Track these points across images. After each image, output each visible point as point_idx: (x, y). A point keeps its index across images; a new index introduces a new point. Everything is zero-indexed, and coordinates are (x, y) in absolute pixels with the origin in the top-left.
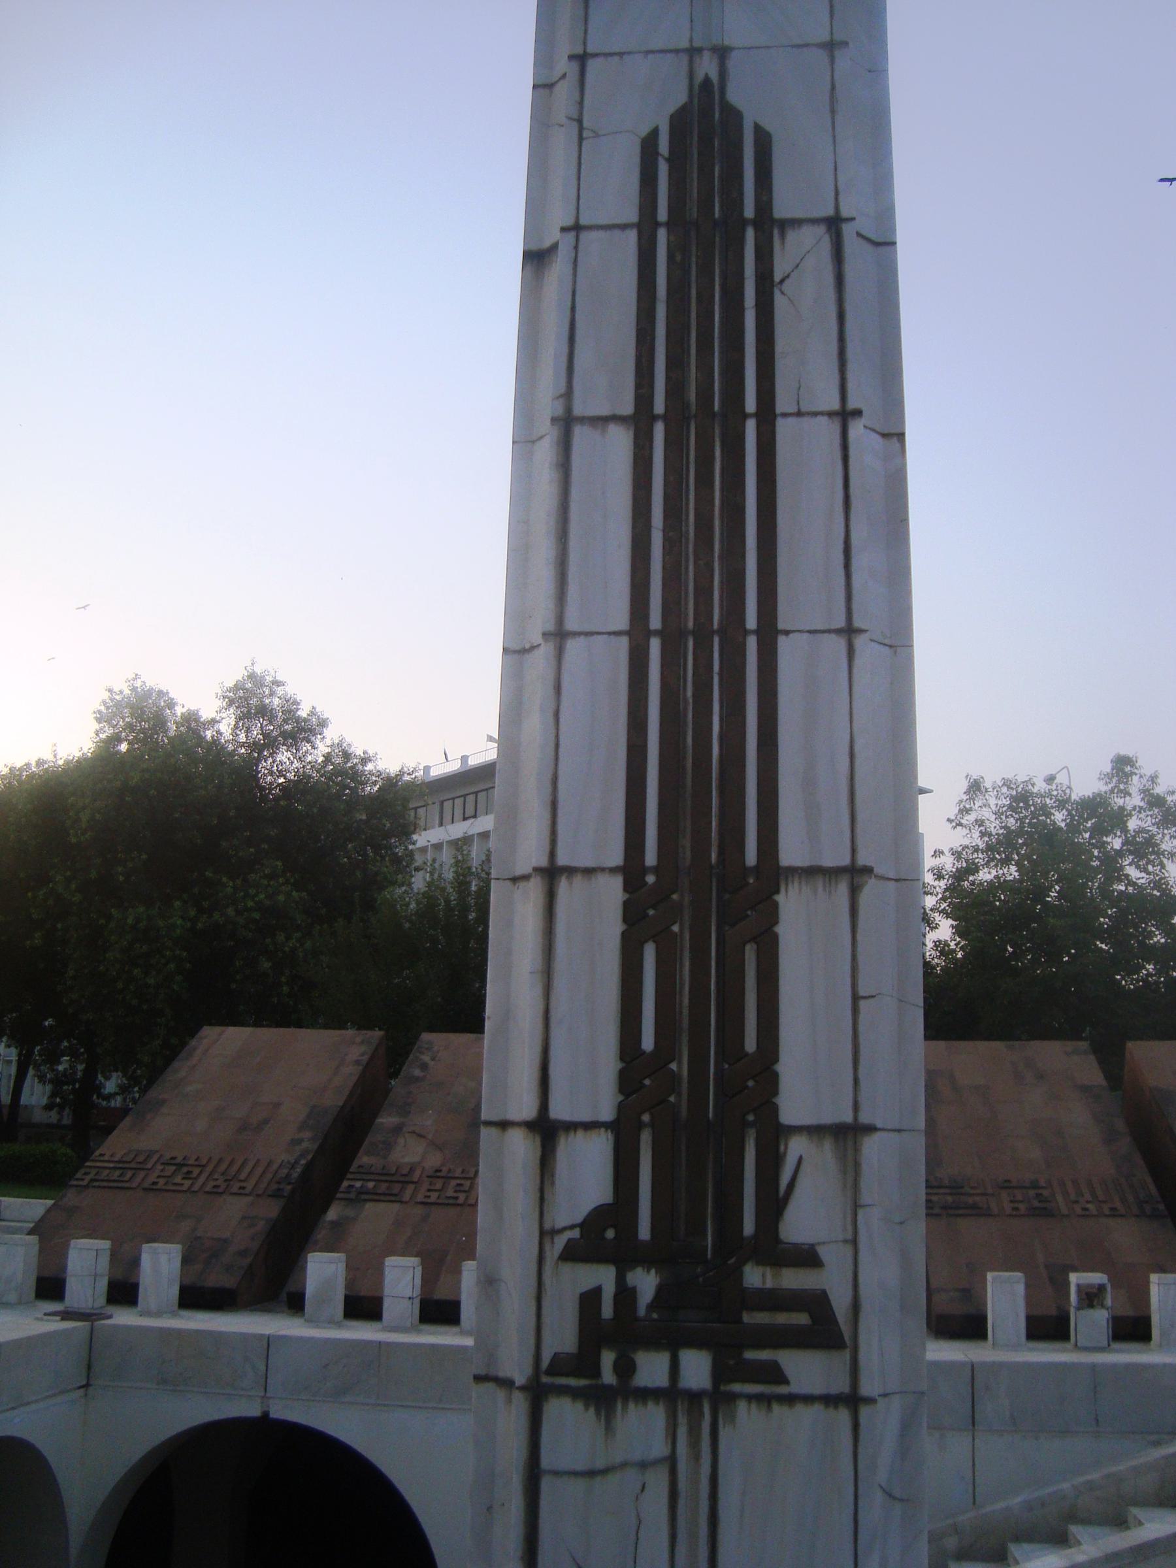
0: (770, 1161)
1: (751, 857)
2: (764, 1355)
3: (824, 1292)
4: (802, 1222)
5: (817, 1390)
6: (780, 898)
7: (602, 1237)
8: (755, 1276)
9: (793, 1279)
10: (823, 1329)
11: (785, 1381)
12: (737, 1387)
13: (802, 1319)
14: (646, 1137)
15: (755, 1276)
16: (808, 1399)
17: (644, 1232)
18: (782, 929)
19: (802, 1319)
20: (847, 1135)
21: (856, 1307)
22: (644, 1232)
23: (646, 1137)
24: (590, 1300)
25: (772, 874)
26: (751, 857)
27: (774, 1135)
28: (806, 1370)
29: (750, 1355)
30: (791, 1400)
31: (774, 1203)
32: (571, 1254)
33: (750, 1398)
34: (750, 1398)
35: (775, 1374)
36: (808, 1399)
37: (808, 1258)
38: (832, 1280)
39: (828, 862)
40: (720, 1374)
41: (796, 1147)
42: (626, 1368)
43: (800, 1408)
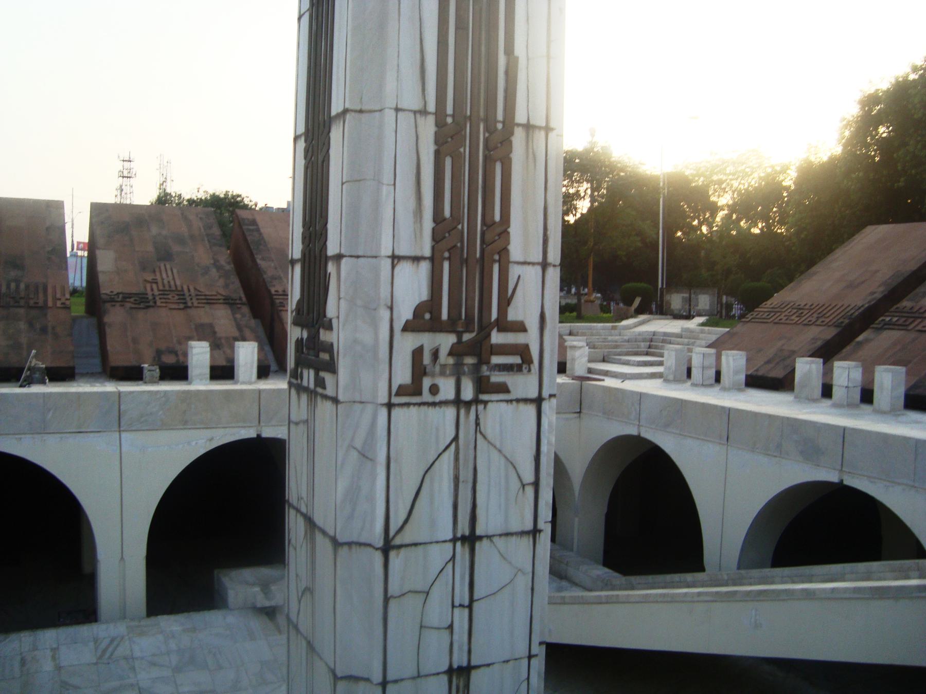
7: (425, 319)
14: (446, 265)
17: (445, 316)
22: (445, 316)
23: (446, 265)
24: (417, 353)
31: (506, 301)
32: (408, 327)
42: (434, 390)
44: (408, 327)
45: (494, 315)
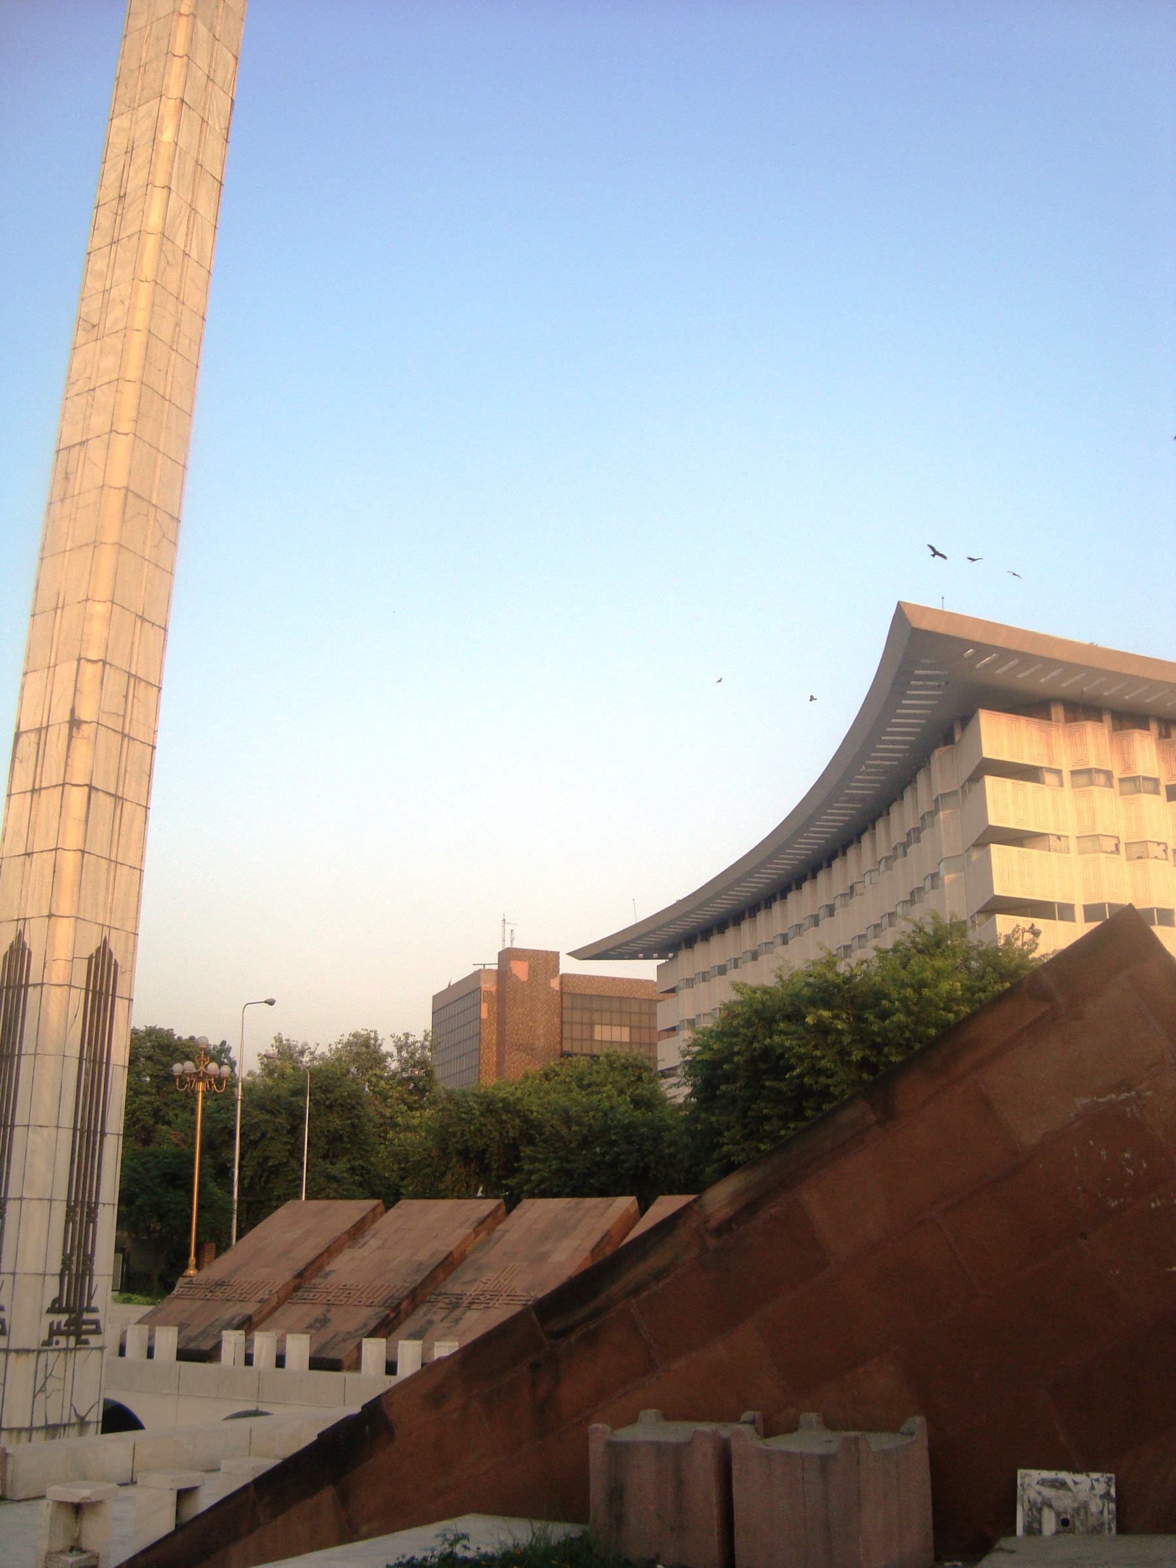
8: (86, 1316)
13: (94, 1327)
19: (94, 1327)
24: (51, 1324)
31: (90, 1297)
37: (95, 1310)
44: (49, 1311)
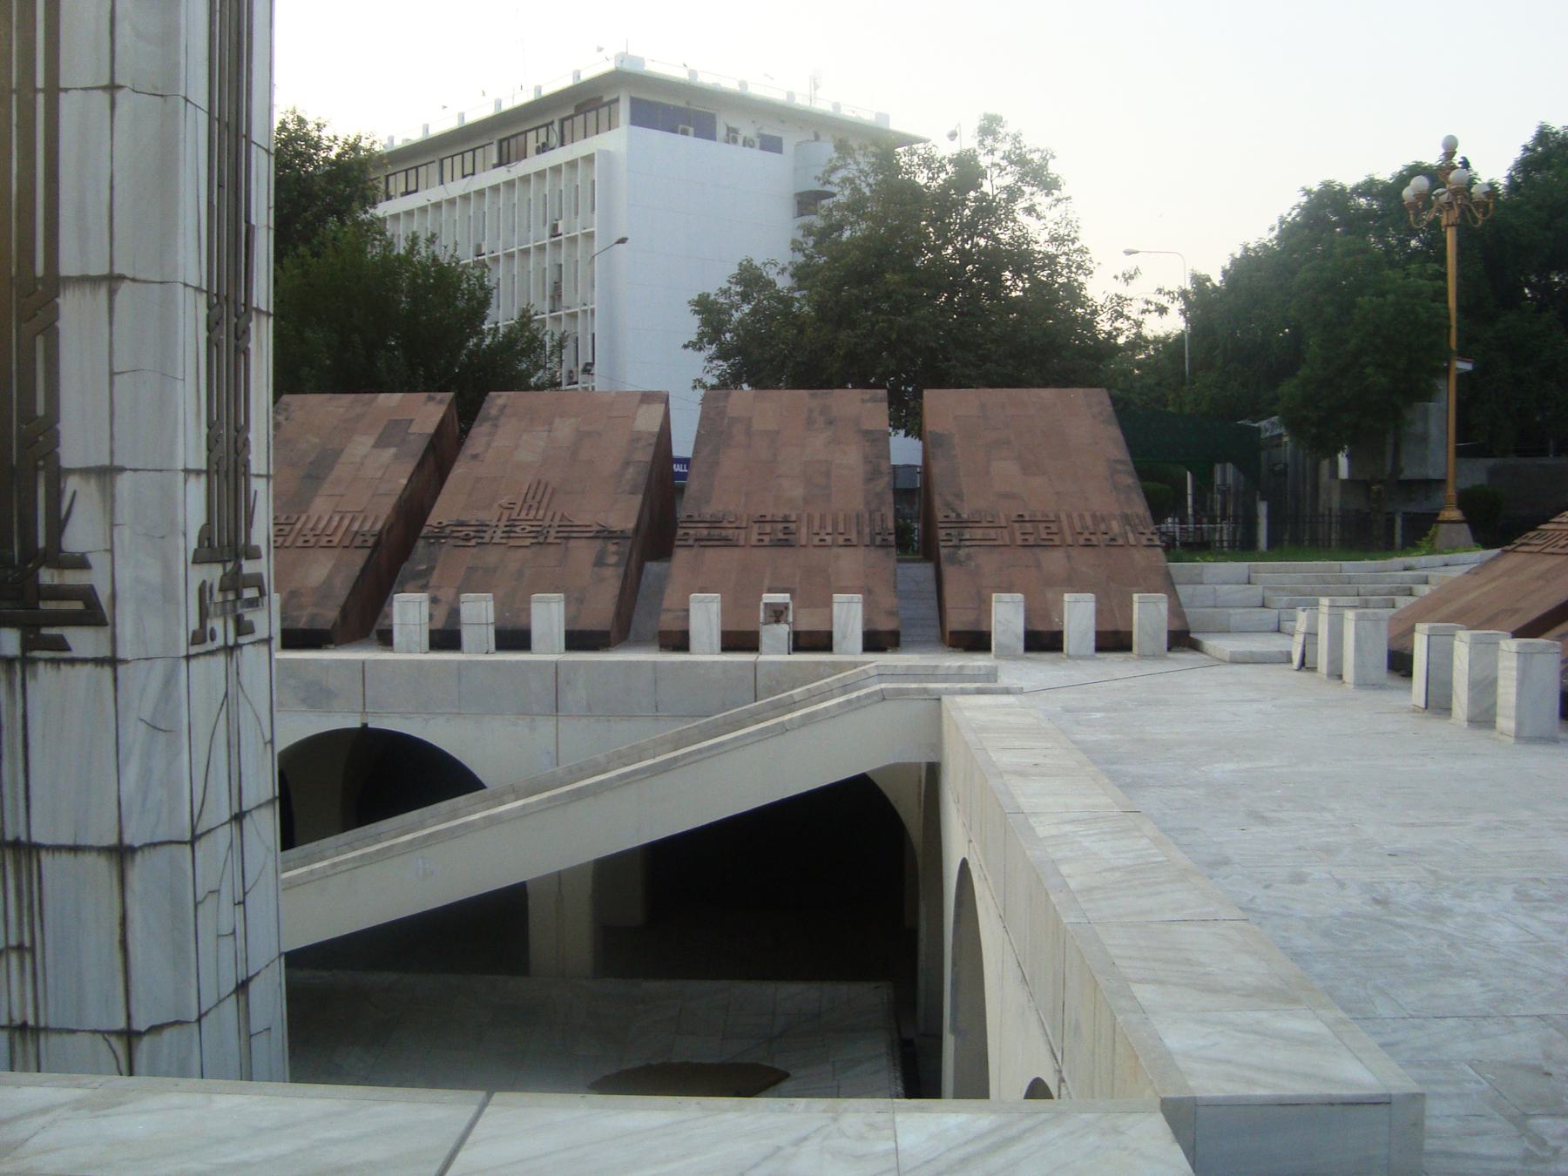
0: (55, 494)
1: (40, 269)
2: (55, 631)
3: (92, 587)
4: (79, 536)
5: (89, 655)
6: (60, 300)
8: (47, 577)
9: (72, 578)
10: (92, 614)
11: (69, 649)
12: (37, 654)
13: (78, 605)
15: (47, 577)
16: (85, 661)
18: (61, 324)
19: (78, 605)
20: (106, 474)
21: (113, 596)
25: (55, 283)
26: (40, 269)
27: (57, 476)
28: (82, 640)
29: (45, 631)
30: (72, 661)
31: (58, 524)
33: (46, 661)
34: (46, 661)
35: (60, 644)
36: (85, 661)
37: (81, 563)
38: (97, 578)
39: (94, 272)
40: (26, 645)
41: (72, 484)
43: (78, 667)
45: (41, 543)
